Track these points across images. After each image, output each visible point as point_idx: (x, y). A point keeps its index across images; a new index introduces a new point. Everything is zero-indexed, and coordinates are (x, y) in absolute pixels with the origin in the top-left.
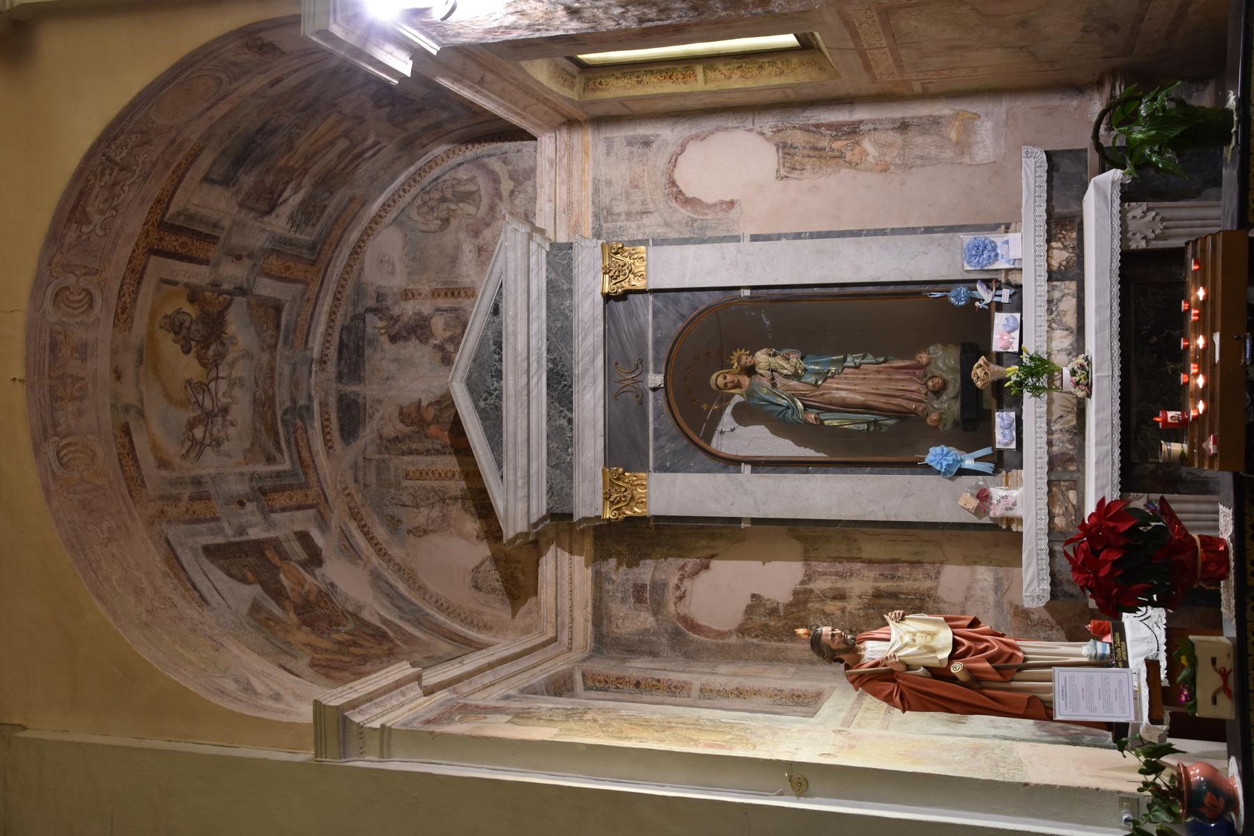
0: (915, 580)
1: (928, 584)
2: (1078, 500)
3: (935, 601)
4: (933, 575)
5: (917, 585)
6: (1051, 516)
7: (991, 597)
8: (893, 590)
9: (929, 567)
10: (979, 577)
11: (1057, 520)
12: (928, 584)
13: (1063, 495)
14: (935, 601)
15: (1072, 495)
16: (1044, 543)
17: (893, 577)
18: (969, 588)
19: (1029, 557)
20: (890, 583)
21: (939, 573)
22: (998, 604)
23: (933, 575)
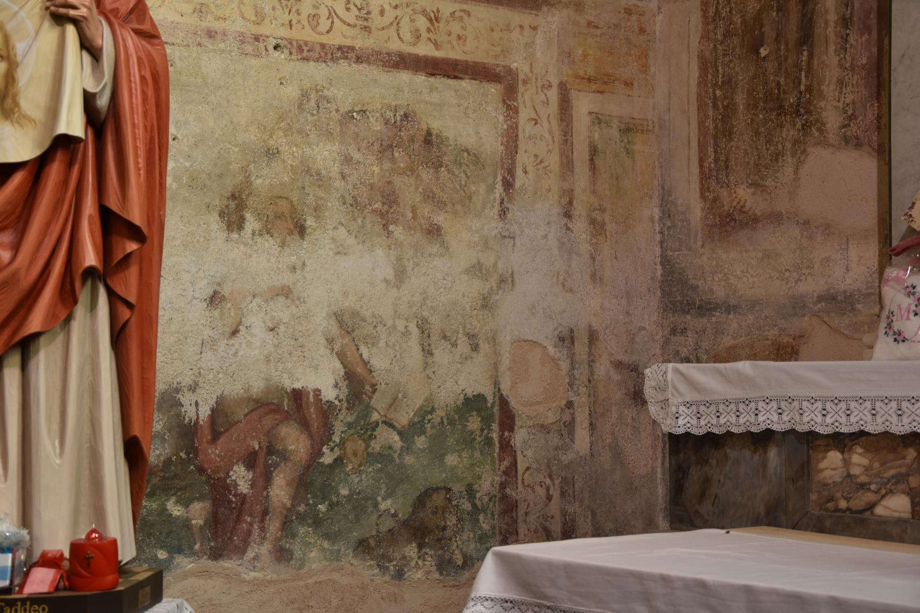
0: (841, 83)
1: (832, 119)
2: (884, 522)
3: (796, 142)
4: (854, 129)
5: (829, 89)
6: (841, 441)
7: (811, 287)
8: (818, 31)
9: (871, 115)
10: (853, 253)
11: (834, 457)
12: (832, 119)
13: (901, 478)
14: (796, 142)
15: (897, 505)
16: (769, 419)
17: (845, 22)
18: (828, 228)
19: (743, 380)
20: (832, 17)
21: (858, 145)
22: (798, 306)
23: (854, 129)
